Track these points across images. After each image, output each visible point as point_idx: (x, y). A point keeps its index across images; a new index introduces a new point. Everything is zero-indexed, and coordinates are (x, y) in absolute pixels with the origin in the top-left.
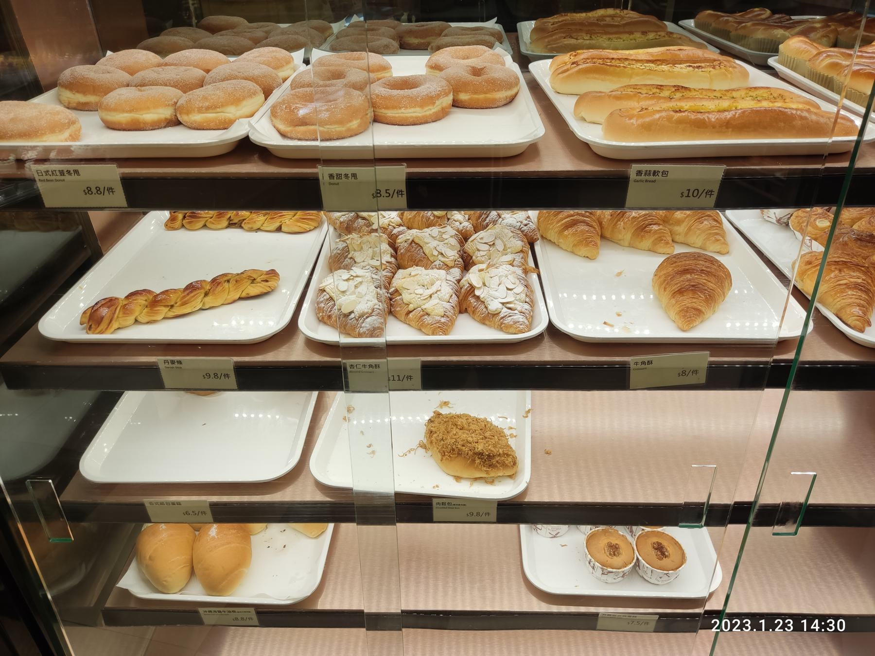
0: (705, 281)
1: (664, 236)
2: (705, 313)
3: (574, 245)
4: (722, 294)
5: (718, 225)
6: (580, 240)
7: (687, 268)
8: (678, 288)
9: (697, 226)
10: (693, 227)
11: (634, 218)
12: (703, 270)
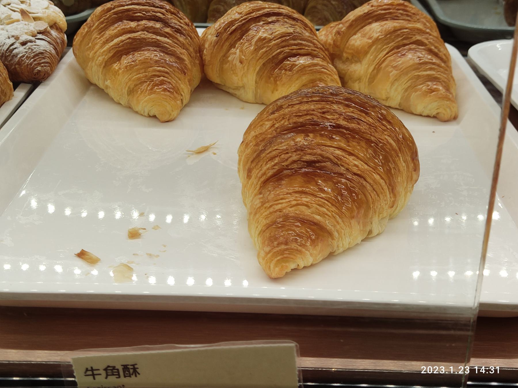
0: (338, 152)
1: (321, 80)
2: (336, 234)
3: (131, 92)
4: (385, 187)
5: (434, 61)
6: (139, 79)
7: (301, 120)
8: (272, 167)
9: (391, 61)
10: (383, 65)
11: (261, 39)
12: (339, 126)
